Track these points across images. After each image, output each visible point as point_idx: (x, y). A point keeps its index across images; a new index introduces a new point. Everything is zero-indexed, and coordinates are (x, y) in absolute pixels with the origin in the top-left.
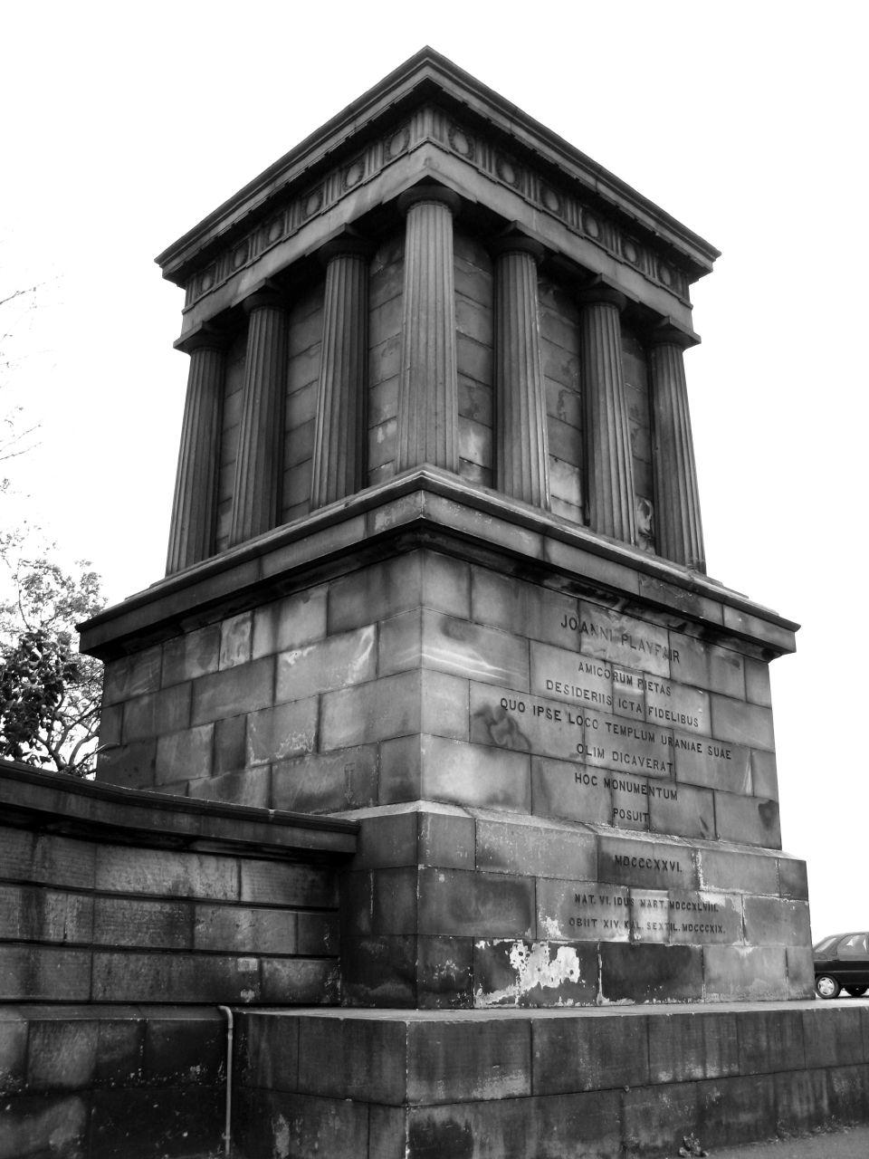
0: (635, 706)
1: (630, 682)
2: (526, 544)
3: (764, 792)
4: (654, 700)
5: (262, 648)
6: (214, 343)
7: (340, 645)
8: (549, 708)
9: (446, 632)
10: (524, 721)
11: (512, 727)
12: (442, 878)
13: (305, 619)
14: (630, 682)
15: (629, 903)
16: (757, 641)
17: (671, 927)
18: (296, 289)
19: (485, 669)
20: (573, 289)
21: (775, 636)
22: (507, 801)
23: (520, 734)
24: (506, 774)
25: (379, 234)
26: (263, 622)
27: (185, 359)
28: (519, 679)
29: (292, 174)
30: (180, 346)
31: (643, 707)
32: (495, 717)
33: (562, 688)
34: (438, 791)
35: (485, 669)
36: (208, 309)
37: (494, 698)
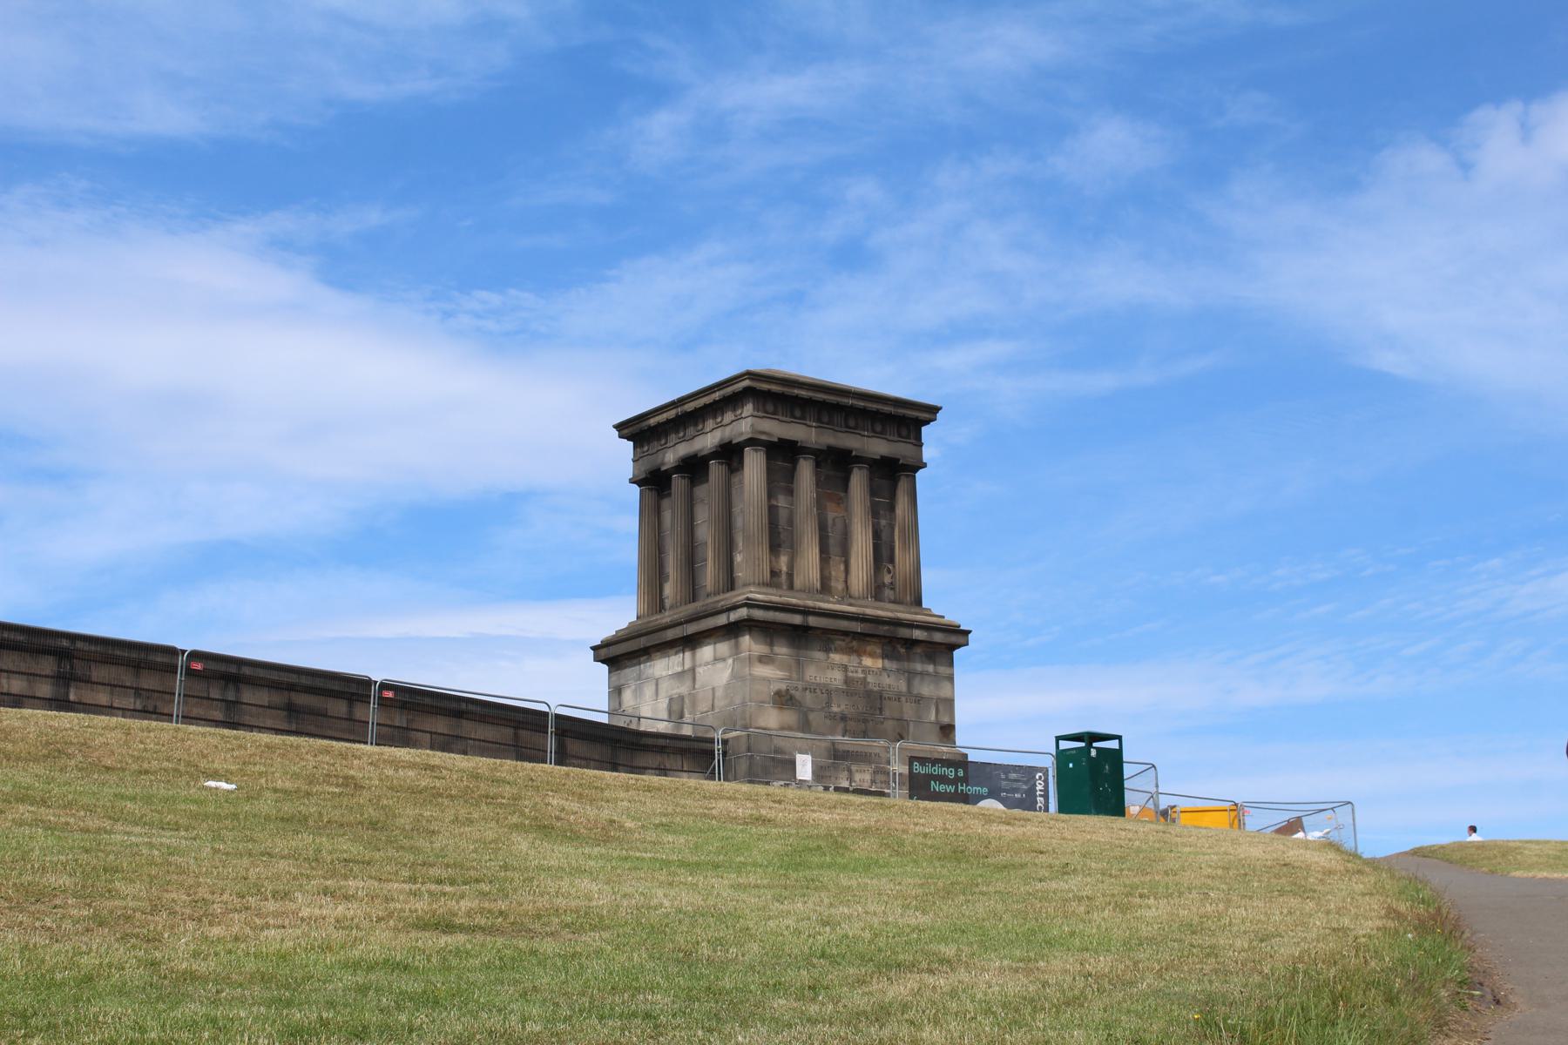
2: (797, 619)
3: (945, 720)
4: (870, 679)
5: (688, 665)
6: (653, 482)
7: (720, 665)
8: (811, 688)
10: (797, 695)
11: (792, 698)
13: (706, 652)
15: (850, 771)
16: (944, 642)
17: (873, 782)
18: (694, 467)
20: (836, 464)
21: (953, 639)
22: (790, 728)
24: (790, 717)
25: (730, 454)
26: (688, 654)
27: (636, 489)
28: (795, 676)
29: (689, 407)
30: (632, 481)
35: (780, 674)
36: (647, 464)
37: (783, 687)
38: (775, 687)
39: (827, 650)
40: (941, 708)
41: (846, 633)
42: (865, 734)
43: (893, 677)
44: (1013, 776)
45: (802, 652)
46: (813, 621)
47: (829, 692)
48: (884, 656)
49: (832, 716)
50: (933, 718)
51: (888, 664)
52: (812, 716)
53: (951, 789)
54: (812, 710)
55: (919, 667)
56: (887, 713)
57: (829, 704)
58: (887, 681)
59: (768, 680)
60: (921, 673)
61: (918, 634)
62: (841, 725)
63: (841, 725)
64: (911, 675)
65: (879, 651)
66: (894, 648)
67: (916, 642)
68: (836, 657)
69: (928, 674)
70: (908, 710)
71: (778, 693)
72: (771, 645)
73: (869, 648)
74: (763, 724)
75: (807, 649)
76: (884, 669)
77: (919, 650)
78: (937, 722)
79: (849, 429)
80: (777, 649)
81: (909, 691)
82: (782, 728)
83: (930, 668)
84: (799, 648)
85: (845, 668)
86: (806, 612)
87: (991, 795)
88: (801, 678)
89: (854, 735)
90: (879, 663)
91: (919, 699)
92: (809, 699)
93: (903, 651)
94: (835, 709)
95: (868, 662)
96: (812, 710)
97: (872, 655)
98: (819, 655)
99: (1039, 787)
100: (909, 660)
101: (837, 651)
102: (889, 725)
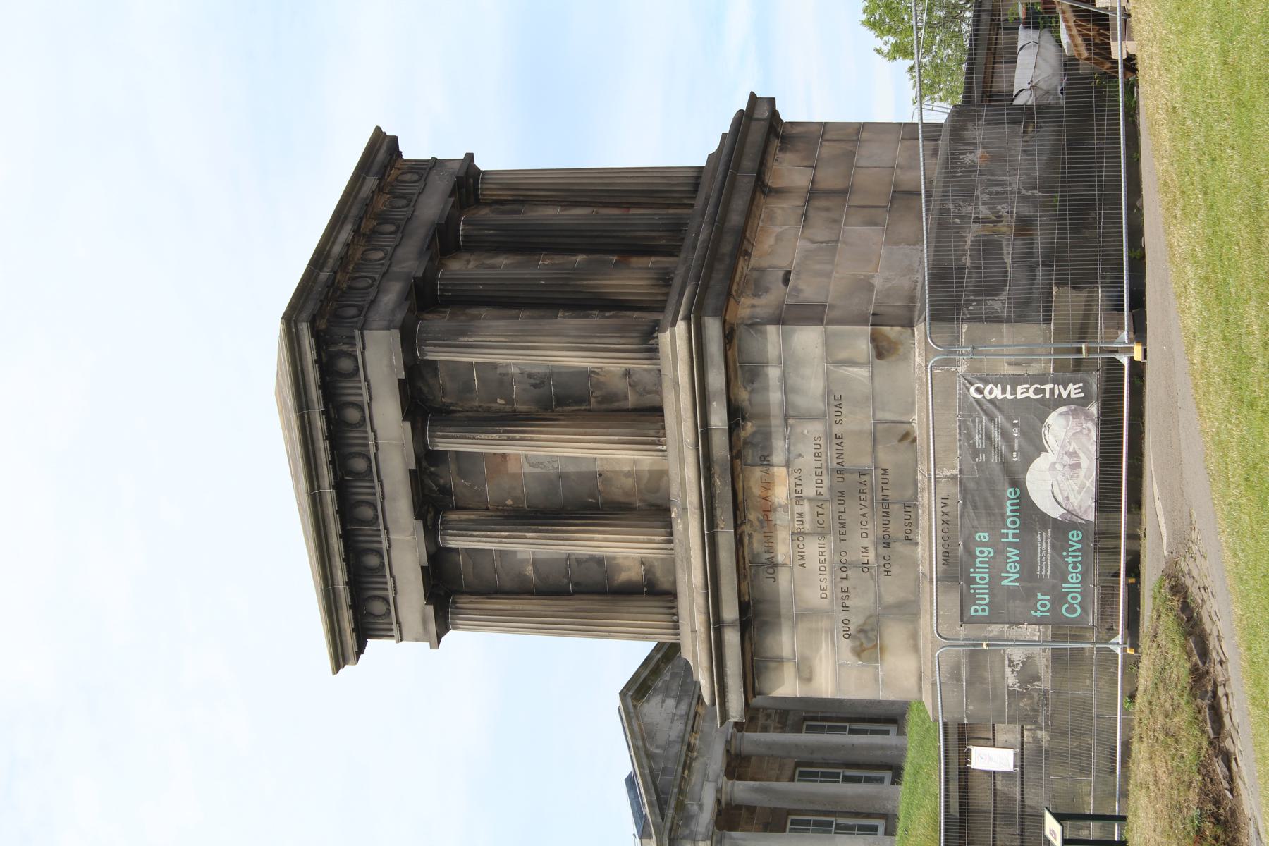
0: (820, 511)
1: (801, 515)
2: (732, 638)
4: (809, 491)
9: (809, 680)
10: (856, 622)
11: (862, 630)
12: (971, 707)
14: (801, 515)
19: (825, 649)
22: (914, 636)
23: (865, 624)
24: (894, 635)
28: (824, 624)
31: (818, 501)
32: (858, 643)
33: (823, 585)
34: (916, 689)
35: (825, 649)
37: (846, 644)
38: (848, 658)
39: (773, 565)
40: (843, 355)
41: (739, 541)
42: (910, 506)
43: (800, 448)
44: (978, 440)
45: (783, 611)
46: (730, 612)
47: (844, 566)
48: (765, 461)
49: (887, 563)
50: (862, 373)
51: (778, 457)
52: (889, 599)
53: (1013, 554)
54: (879, 597)
55: (775, 397)
56: (866, 462)
57: (865, 567)
58: (808, 461)
59: (839, 667)
60: (786, 391)
61: (718, 418)
62: (899, 547)
63: (899, 547)
64: (791, 414)
65: (757, 472)
66: (746, 443)
67: (736, 415)
68: (783, 551)
69: (784, 379)
70: (855, 421)
71: (858, 652)
72: (780, 661)
73: (757, 491)
74: (913, 681)
75: (776, 602)
76: (788, 464)
77: (743, 396)
78: (870, 364)
79: (371, 473)
80: (786, 652)
81: (823, 416)
82: (916, 649)
83: (774, 373)
84: (778, 616)
85: (799, 535)
86: (716, 626)
87: (1017, 483)
88: (828, 614)
89: (911, 524)
90: (780, 472)
91: (834, 400)
92: (861, 602)
93: (750, 427)
94: (872, 557)
95: (781, 494)
96: (879, 597)
97: (768, 485)
98: (783, 578)
99: (997, 393)
100: (766, 416)
101: (770, 549)
102: (887, 458)
